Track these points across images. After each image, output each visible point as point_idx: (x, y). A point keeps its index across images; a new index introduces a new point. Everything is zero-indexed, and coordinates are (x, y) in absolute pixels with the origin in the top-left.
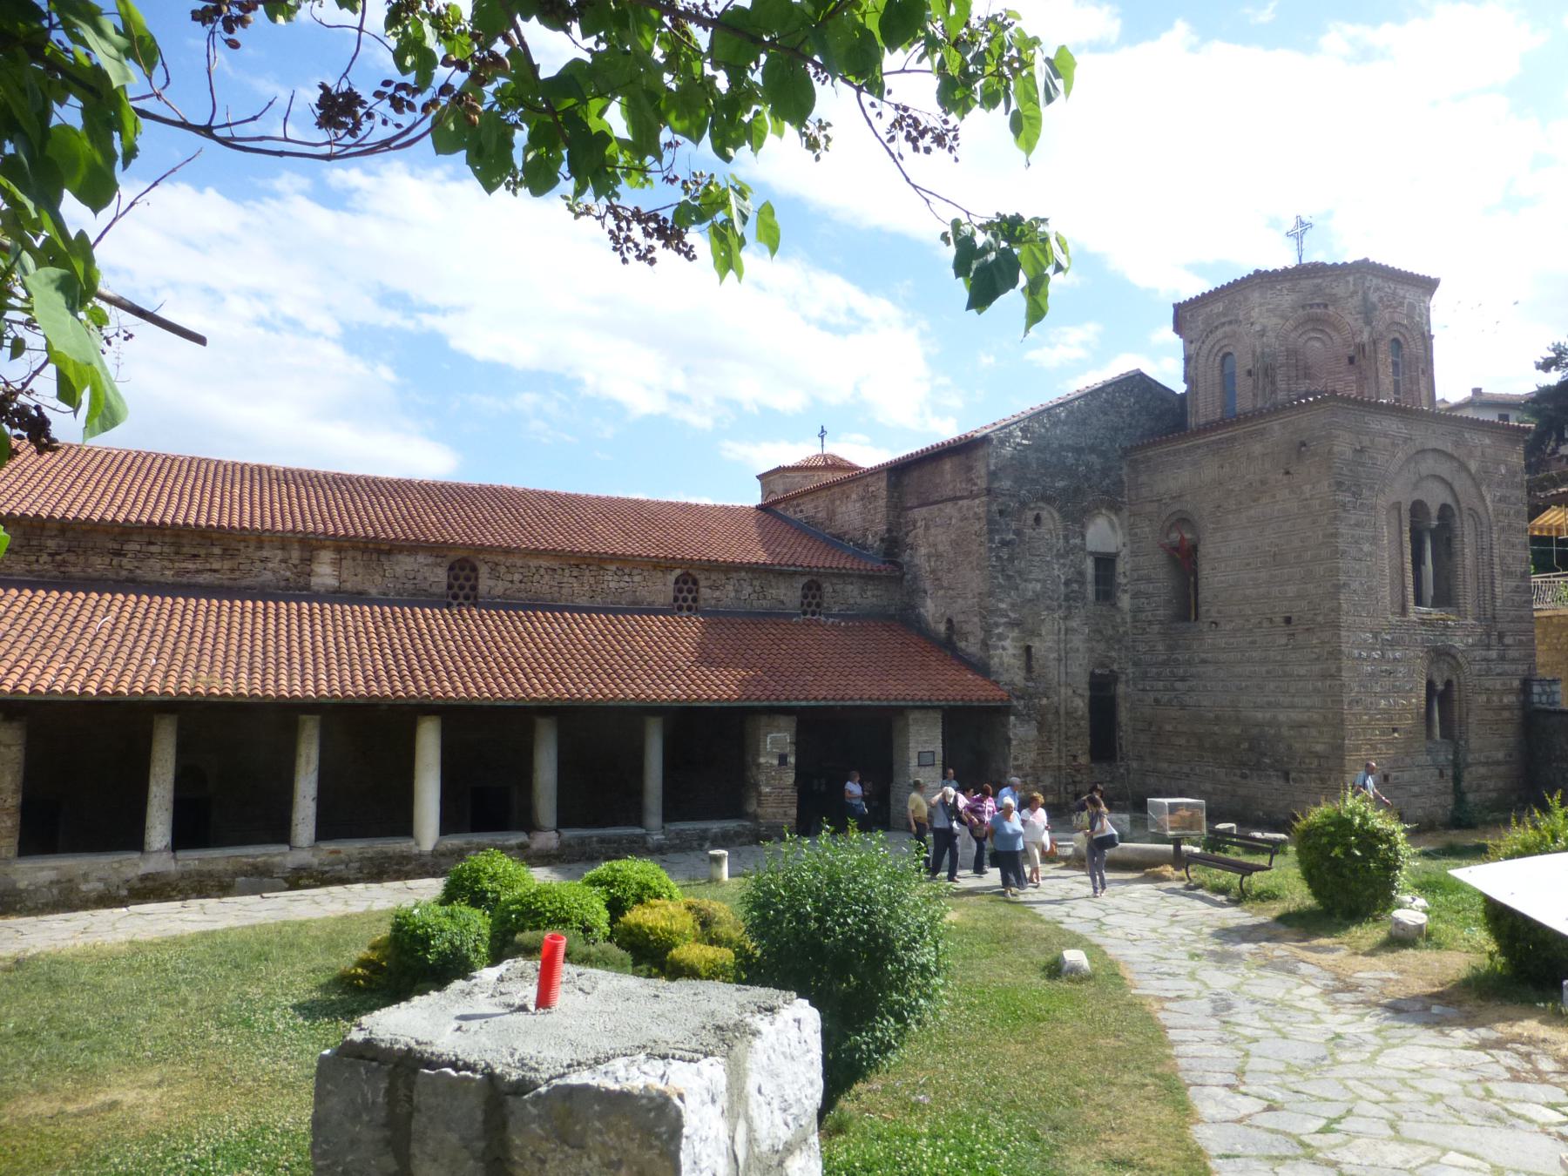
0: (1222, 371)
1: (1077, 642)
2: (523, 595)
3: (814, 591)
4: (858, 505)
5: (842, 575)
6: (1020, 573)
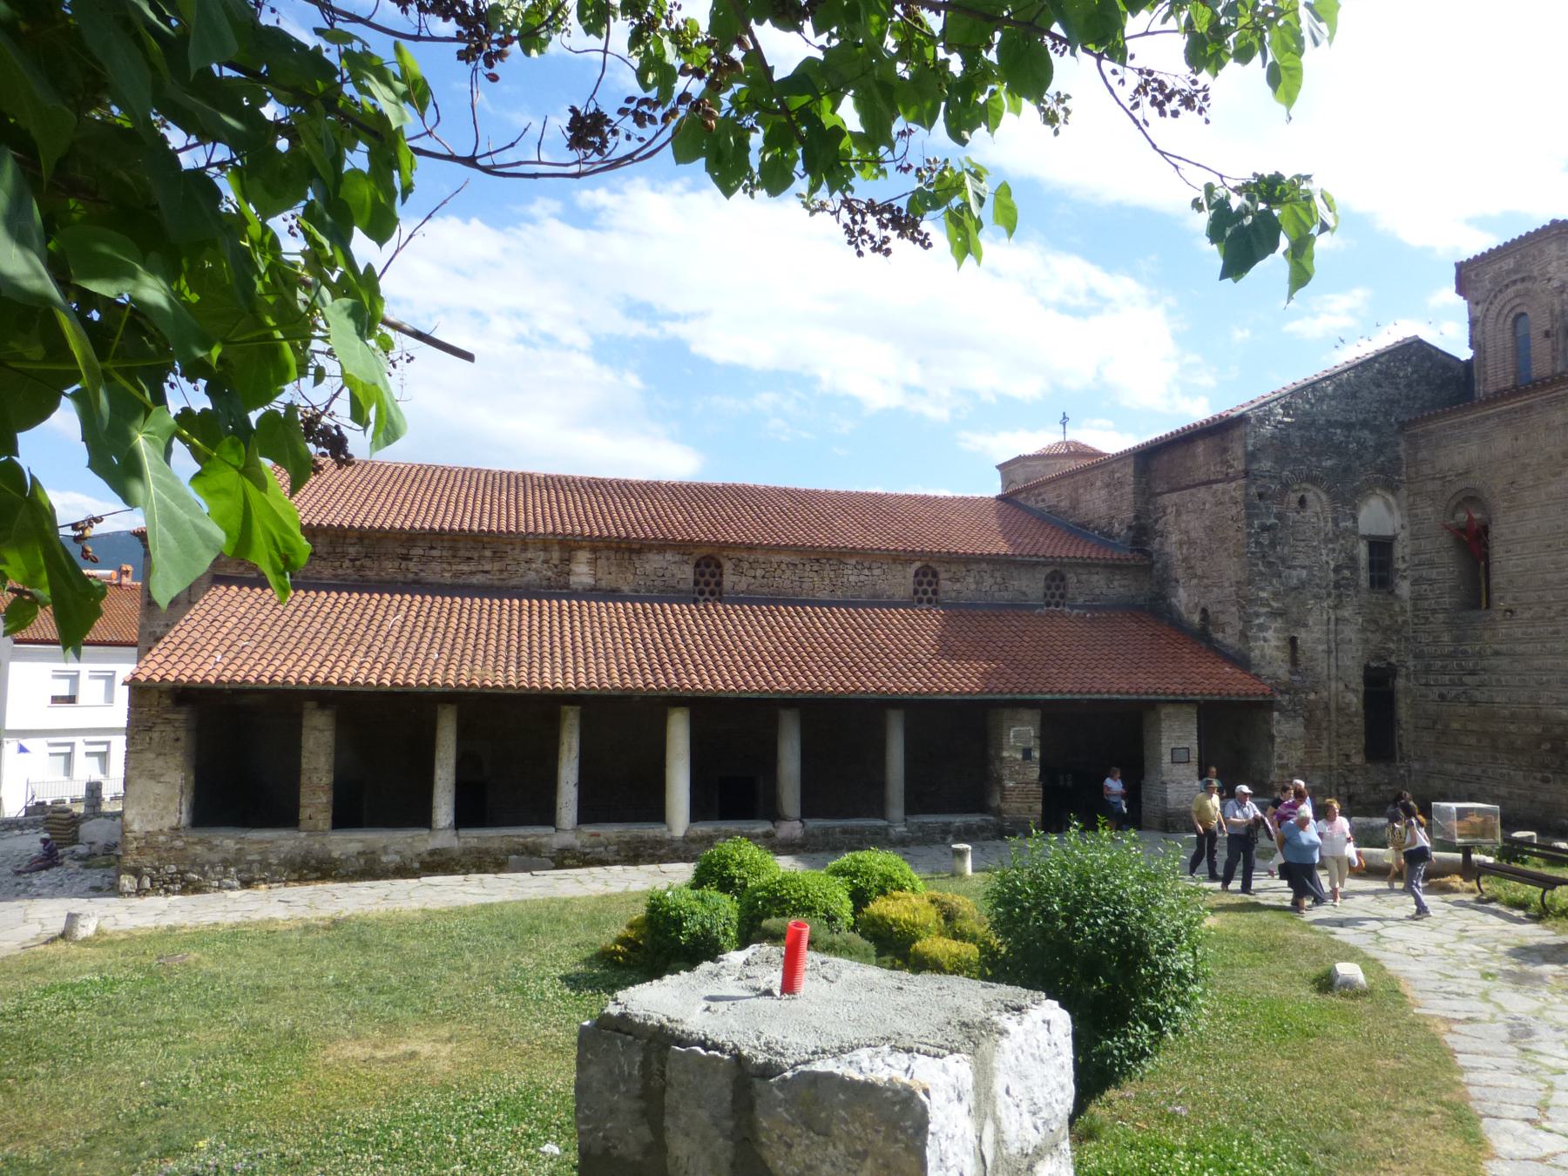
0: (1514, 334)
1: (1349, 632)
2: (766, 590)
3: (1057, 582)
4: (1103, 492)
5: (1087, 565)
6: (1283, 560)
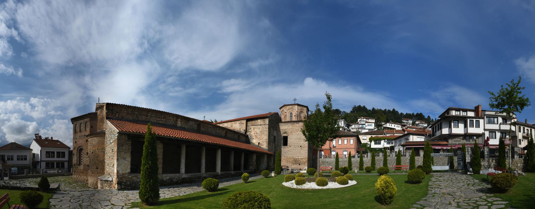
2: (207, 131)
